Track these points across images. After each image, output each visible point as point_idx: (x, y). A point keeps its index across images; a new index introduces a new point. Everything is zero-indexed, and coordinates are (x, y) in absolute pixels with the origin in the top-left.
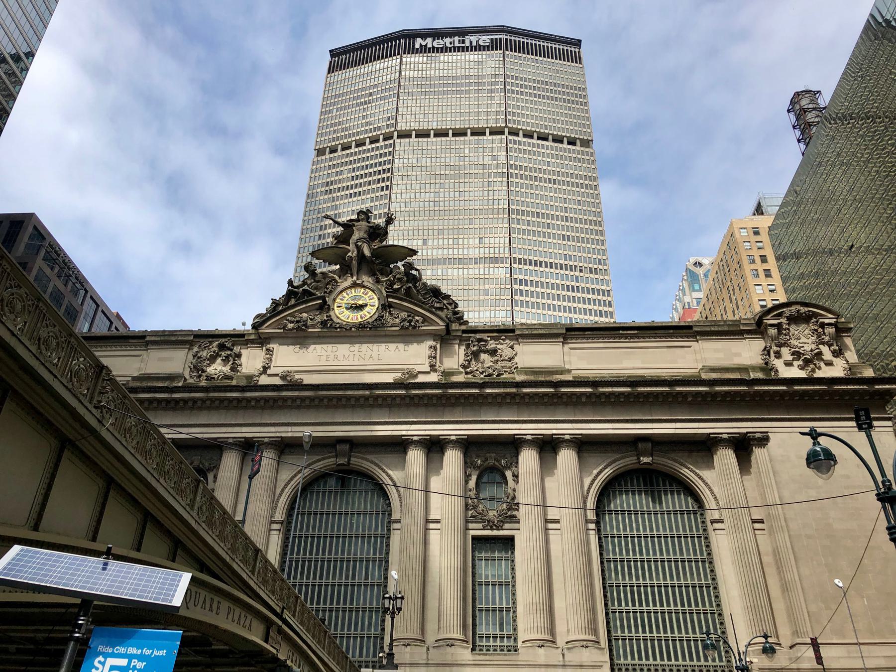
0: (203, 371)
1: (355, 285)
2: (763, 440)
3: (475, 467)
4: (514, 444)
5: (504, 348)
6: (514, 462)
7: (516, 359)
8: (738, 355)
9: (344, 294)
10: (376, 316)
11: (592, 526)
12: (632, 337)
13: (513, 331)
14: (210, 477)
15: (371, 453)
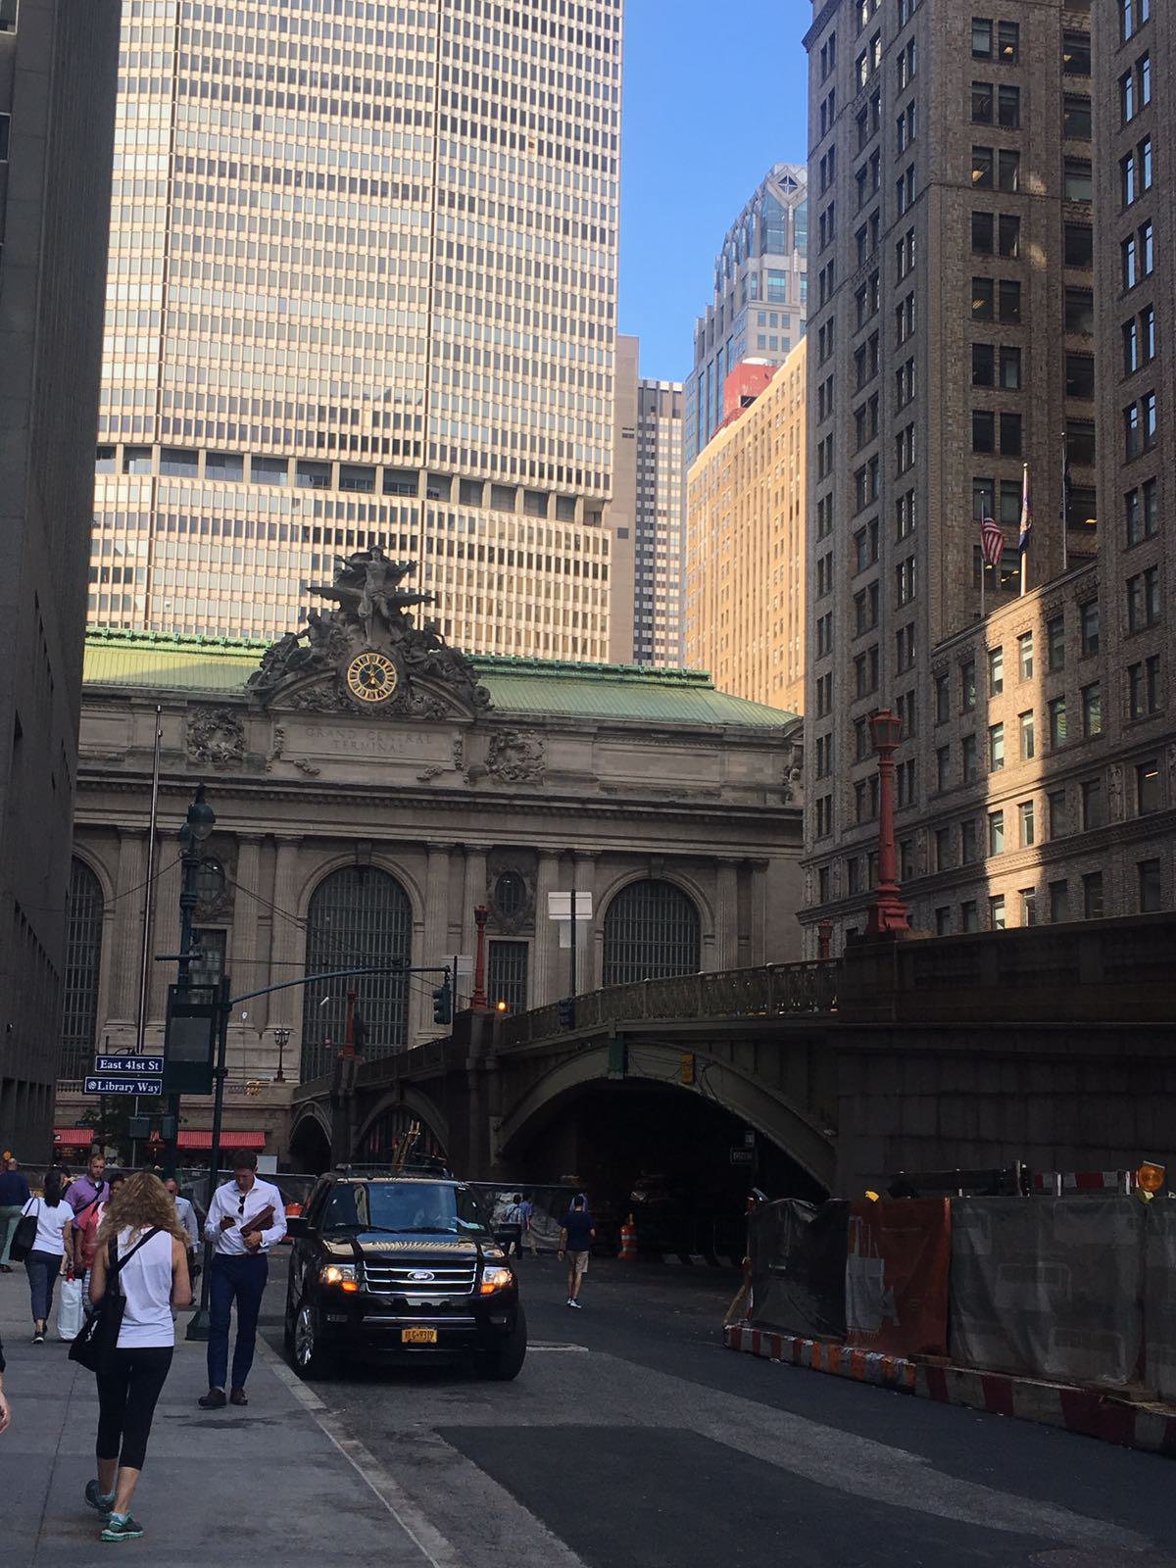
0: (205, 747)
1: (370, 650)
2: (763, 865)
3: (496, 873)
4: (538, 854)
5: (532, 741)
6: (534, 875)
7: (544, 758)
8: (761, 770)
9: (357, 660)
10: (395, 697)
11: (601, 936)
12: (664, 740)
13: (543, 725)
14: (227, 868)
15: (392, 853)
